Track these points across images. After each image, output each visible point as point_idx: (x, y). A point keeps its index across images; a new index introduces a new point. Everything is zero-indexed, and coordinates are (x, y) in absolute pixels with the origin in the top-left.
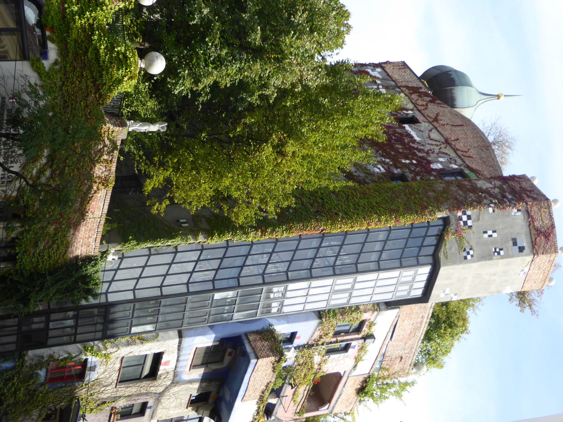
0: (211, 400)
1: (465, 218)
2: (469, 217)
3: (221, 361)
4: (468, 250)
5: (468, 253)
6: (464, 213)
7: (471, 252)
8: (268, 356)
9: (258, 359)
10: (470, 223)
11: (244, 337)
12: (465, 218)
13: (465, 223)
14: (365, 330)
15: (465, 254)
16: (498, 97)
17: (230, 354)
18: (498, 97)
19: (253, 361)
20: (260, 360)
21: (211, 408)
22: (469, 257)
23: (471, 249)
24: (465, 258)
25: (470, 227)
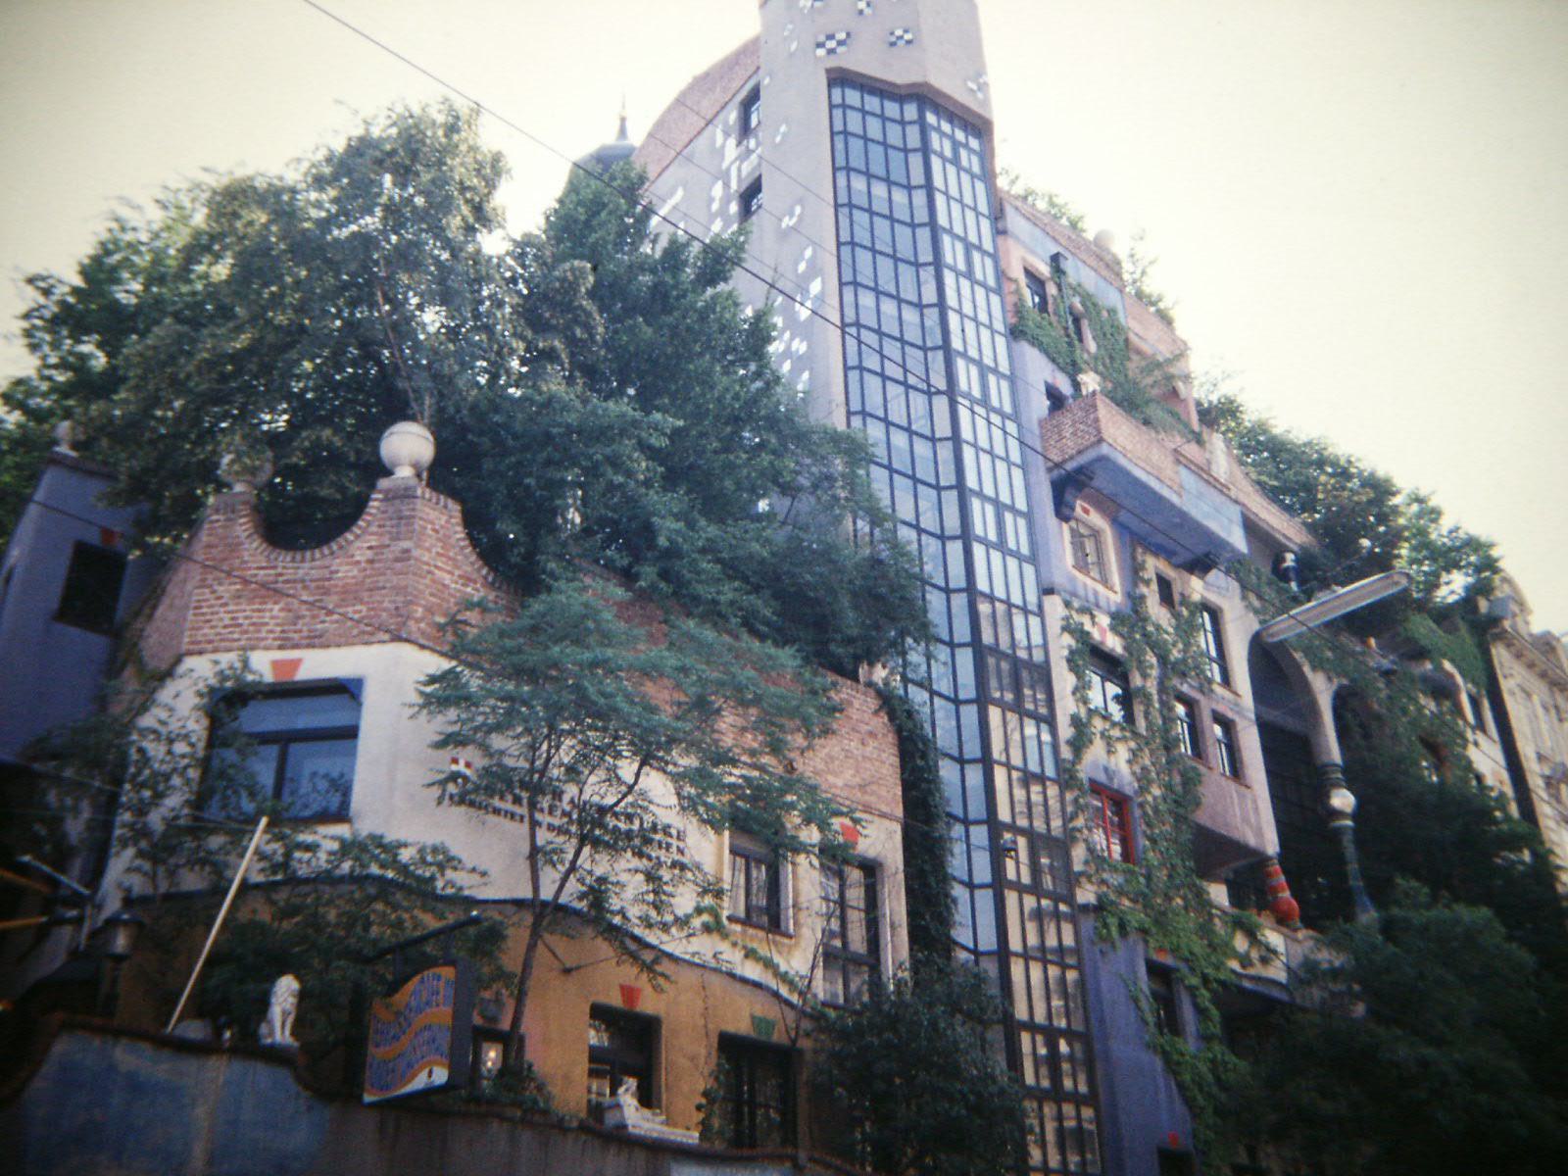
0: (1170, 573)
1: (831, 44)
2: (831, 37)
3: (1096, 534)
4: (893, 39)
5: (900, 38)
6: (820, 45)
7: (899, 32)
8: (1097, 420)
9: (1101, 440)
10: (842, 36)
11: (1056, 473)
12: (831, 44)
13: (841, 43)
14: (1044, 269)
15: (901, 43)
16: (623, 120)
17: (1086, 511)
18: (623, 120)
19: (1105, 449)
20: (1105, 437)
21: (1186, 575)
22: (908, 37)
23: (892, 34)
24: (909, 42)
25: (848, 35)
